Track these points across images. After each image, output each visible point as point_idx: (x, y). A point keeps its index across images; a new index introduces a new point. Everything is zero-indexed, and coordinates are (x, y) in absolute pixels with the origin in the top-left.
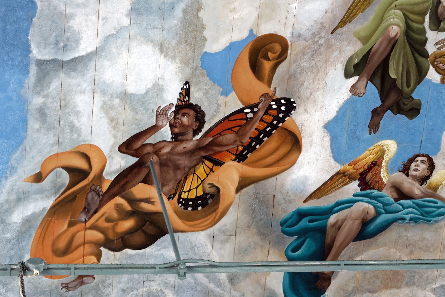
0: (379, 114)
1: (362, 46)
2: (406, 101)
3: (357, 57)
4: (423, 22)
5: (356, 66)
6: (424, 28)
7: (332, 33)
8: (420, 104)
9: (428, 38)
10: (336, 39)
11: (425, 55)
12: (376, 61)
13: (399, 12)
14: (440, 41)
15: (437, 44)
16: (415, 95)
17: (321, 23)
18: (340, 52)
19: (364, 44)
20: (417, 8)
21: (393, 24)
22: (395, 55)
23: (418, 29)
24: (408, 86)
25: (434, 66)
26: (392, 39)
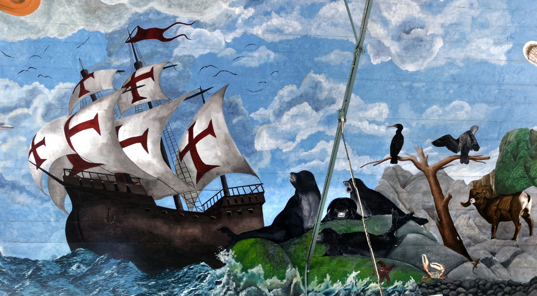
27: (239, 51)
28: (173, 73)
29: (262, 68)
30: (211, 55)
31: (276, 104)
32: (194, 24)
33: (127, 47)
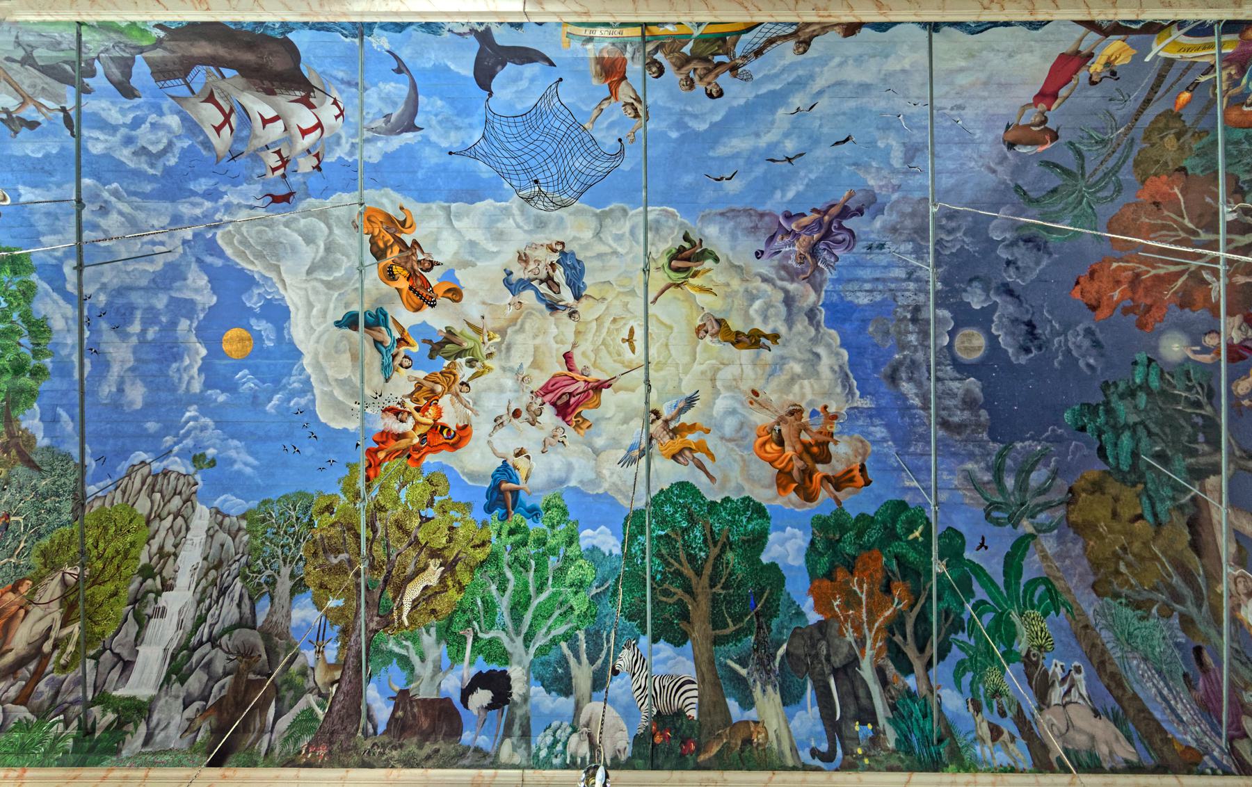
27: (216, 189)
28: (258, 171)
29: (196, 177)
30: (235, 185)
31: (177, 151)
32: (252, 208)
33: (294, 189)
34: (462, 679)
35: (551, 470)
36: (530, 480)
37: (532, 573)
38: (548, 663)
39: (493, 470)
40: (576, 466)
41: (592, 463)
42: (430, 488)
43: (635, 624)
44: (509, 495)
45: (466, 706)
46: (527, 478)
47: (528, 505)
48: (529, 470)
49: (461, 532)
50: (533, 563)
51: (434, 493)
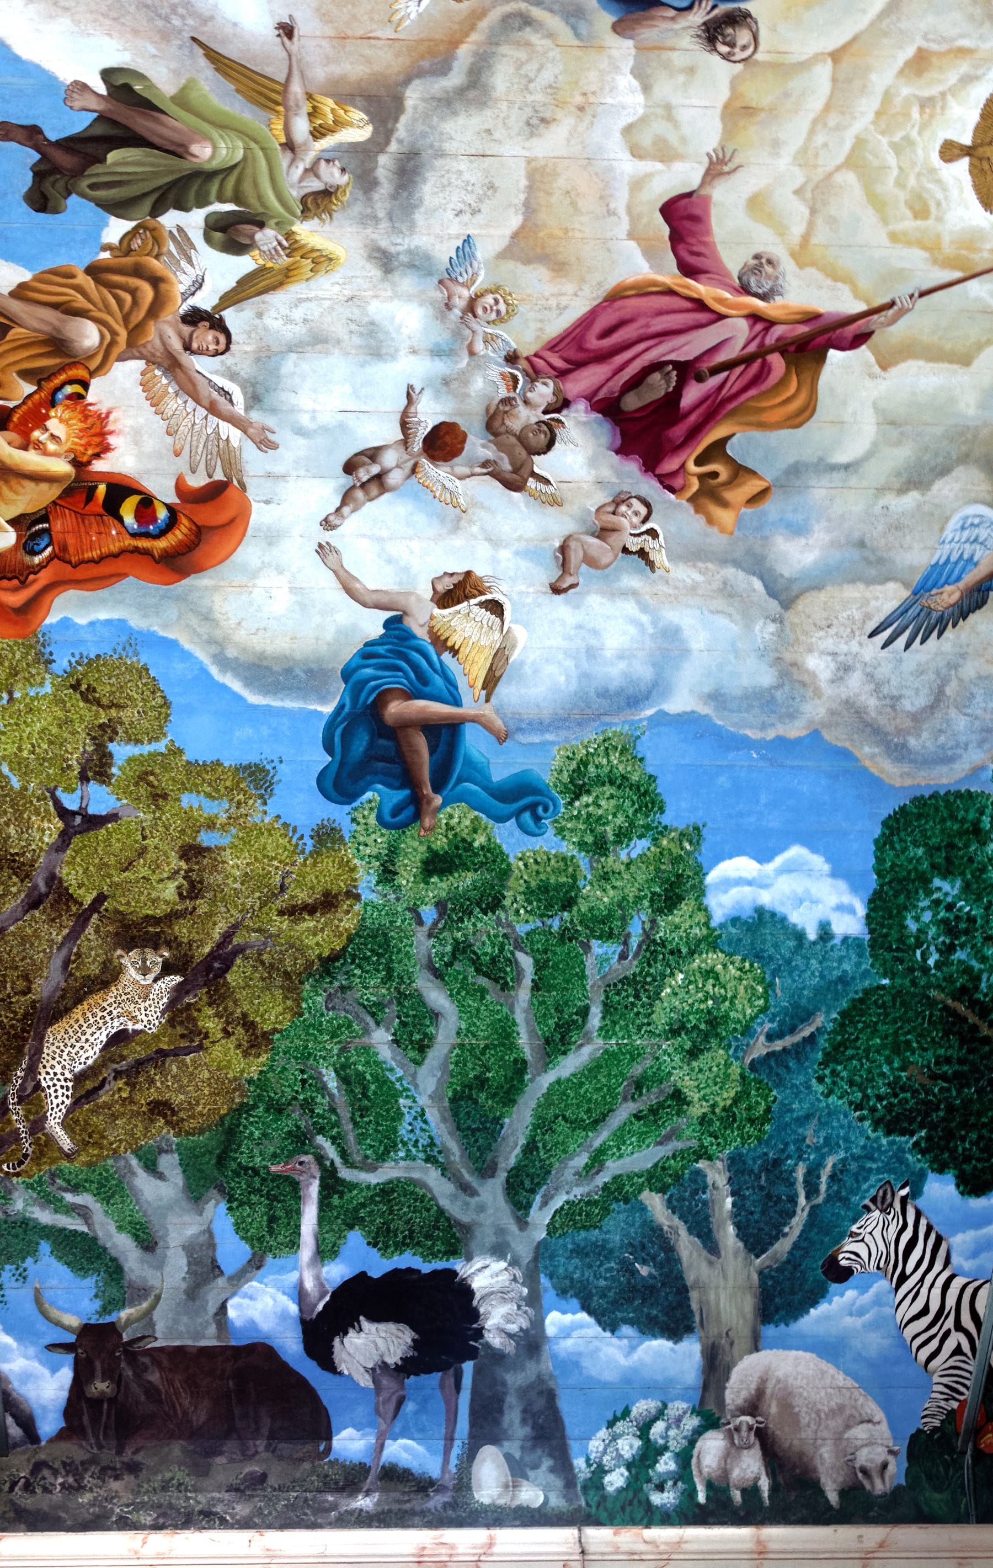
0: (30, 138)
1: (168, 96)
2: (60, 185)
3: (146, 87)
4: (221, 200)
5: (127, 88)
6: (209, 203)
7: (194, 39)
8: (56, 211)
9: (191, 213)
10: (180, 47)
11: (157, 210)
12: (141, 123)
13: (239, 155)
14: (186, 235)
15: (180, 229)
16: (74, 200)
17: (212, 18)
18: (154, 56)
19: (173, 99)
20: (247, 187)
21: (215, 148)
22: (155, 156)
23: (207, 194)
24: (93, 187)
25: (135, 229)
26: (184, 146)
34: (300, 1295)
35: (592, 653)
36: (504, 691)
37: (524, 994)
38: (602, 1251)
39: (348, 653)
40: (697, 640)
41: (765, 631)
42: (85, 715)
43: (907, 1141)
44: (421, 743)
45: (328, 1364)
46: (491, 682)
47: (499, 774)
48: (500, 655)
49: (235, 864)
50: (526, 962)
51: (106, 732)
